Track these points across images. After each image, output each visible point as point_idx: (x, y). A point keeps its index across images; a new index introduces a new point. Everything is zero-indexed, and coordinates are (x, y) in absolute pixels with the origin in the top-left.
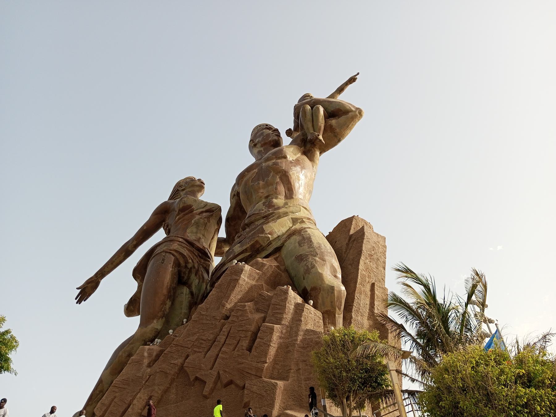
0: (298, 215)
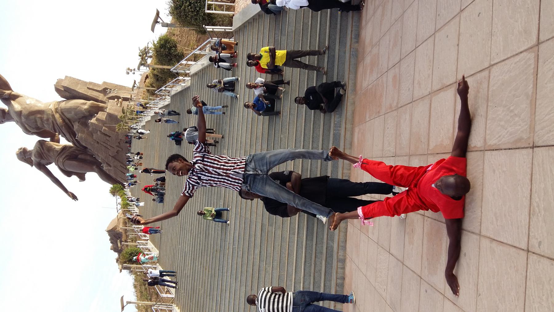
0: (53, 110)
